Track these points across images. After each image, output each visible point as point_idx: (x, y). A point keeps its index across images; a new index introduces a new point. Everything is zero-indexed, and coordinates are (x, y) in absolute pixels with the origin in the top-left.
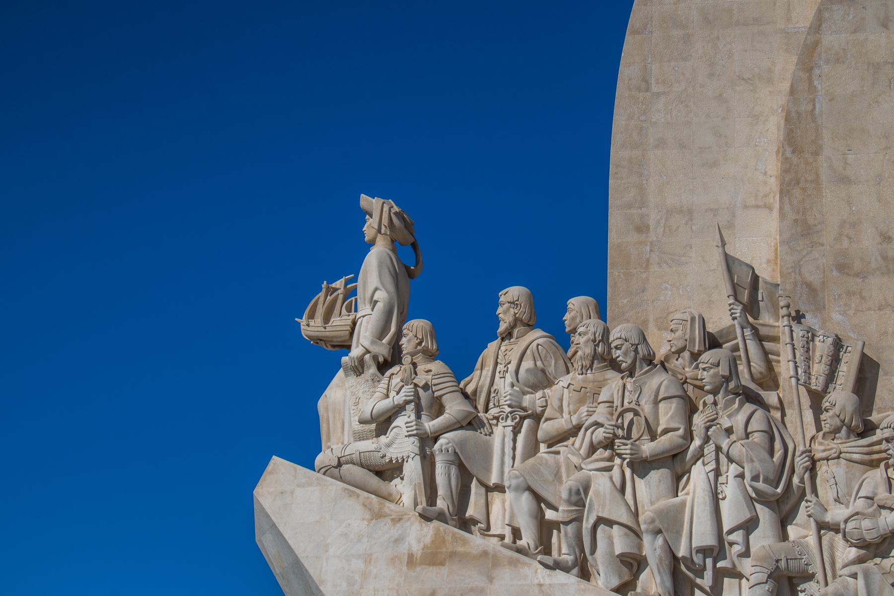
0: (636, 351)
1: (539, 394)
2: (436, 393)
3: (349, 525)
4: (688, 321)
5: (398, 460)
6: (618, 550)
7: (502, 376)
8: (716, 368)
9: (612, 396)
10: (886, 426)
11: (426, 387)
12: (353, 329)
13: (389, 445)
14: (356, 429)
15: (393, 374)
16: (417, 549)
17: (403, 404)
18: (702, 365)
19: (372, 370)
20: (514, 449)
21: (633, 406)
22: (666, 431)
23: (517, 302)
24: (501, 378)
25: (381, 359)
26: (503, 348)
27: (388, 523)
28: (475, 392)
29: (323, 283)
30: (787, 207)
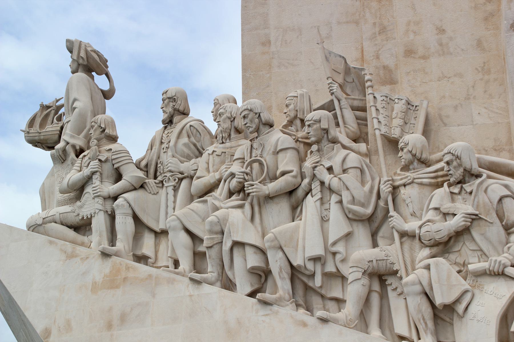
1: (193, 161)
2: (115, 166)
3: (49, 265)
4: (297, 97)
6: (249, 266)
7: (165, 151)
8: (318, 123)
10: (447, 152)
11: (106, 161)
12: (61, 133)
13: (81, 207)
14: (59, 199)
15: (85, 156)
18: (308, 123)
20: (175, 202)
22: (283, 174)
23: (174, 97)
24: (164, 152)
25: (78, 148)
26: (166, 132)
27: (79, 262)
28: (147, 166)
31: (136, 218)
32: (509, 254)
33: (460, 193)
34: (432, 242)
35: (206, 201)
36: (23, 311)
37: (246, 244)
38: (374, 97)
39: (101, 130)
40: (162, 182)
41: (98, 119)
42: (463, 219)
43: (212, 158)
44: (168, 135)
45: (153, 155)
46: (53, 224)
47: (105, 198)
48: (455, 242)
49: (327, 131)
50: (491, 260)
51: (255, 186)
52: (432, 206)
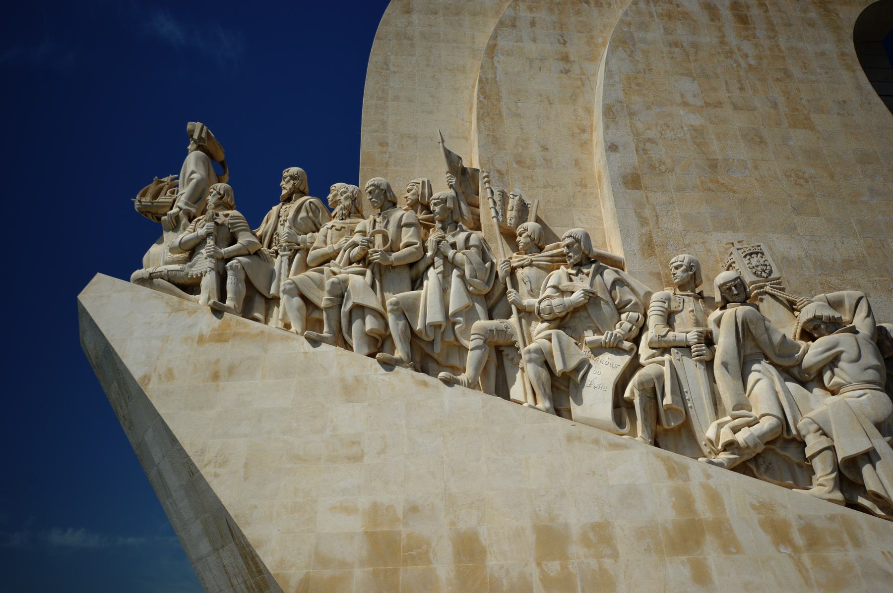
1: (310, 234)
2: (231, 230)
3: (153, 317)
4: (419, 184)
7: (282, 223)
9: (365, 227)
10: (568, 235)
11: (223, 225)
13: (191, 267)
14: (168, 260)
15: (199, 220)
16: (206, 331)
19: (184, 220)
21: (383, 229)
29: (155, 177)
30: (483, 127)
31: (248, 282)
32: (622, 329)
35: (322, 272)
36: (121, 358)
37: (366, 307)
38: (492, 192)
39: (219, 196)
42: (583, 295)
43: (331, 232)
45: (269, 227)
46: (160, 279)
47: (218, 259)
48: (571, 318)
50: (608, 333)
51: (380, 252)
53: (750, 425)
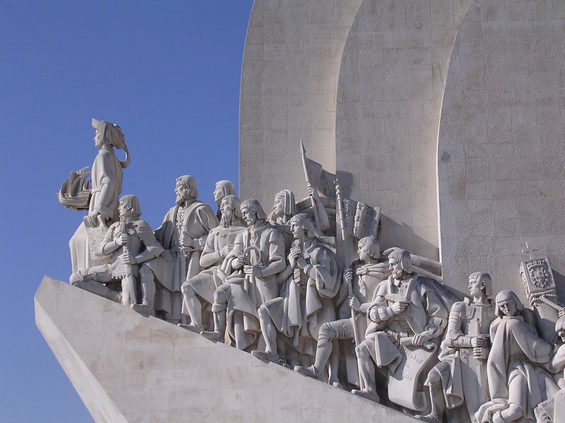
0: (256, 214)
5: (119, 278)
11: (134, 235)
12: (90, 199)
13: (114, 269)
17: (121, 245)
19: (102, 224)
21: (254, 246)
22: (273, 261)
23: (187, 185)
25: (108, 219)
31: (156, 280)
33: (399, 286)
34: (378, 321)
35: (211, 273)
39: (128, 208)
40: (176, 252)
41: (126, 199)
43: (217, 238)
44: (181, 215)
49: (307, 230)
50: (416, 336)
52: (379, 293)
53: (501, 410)
